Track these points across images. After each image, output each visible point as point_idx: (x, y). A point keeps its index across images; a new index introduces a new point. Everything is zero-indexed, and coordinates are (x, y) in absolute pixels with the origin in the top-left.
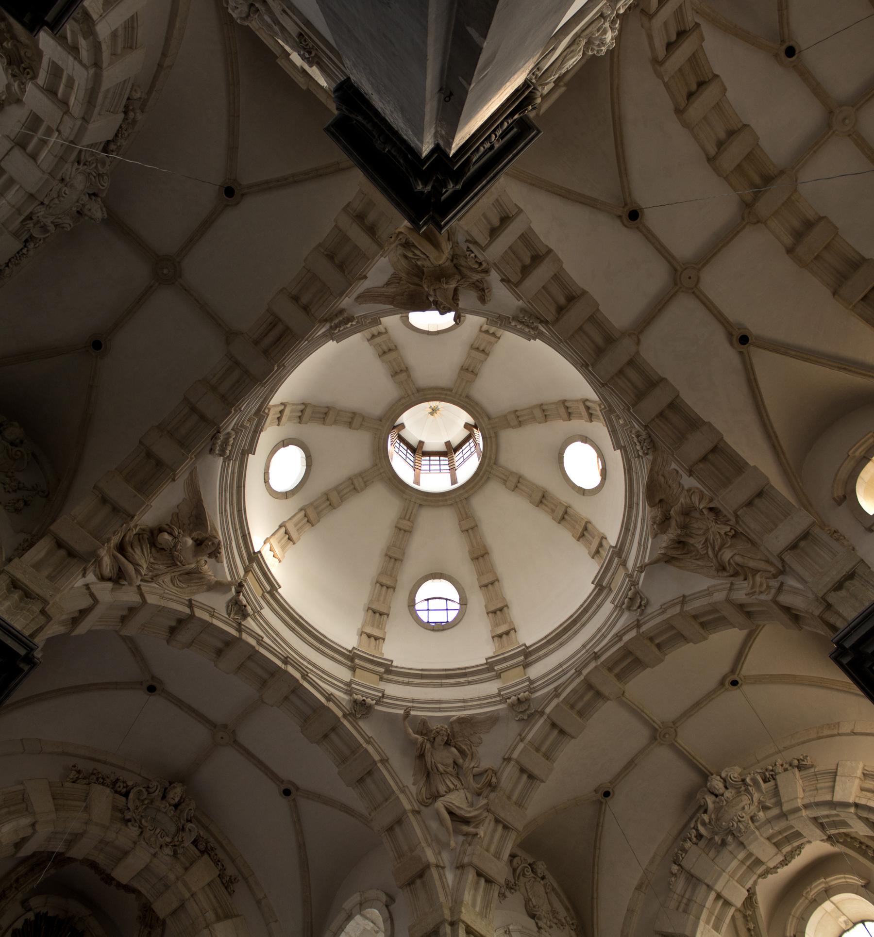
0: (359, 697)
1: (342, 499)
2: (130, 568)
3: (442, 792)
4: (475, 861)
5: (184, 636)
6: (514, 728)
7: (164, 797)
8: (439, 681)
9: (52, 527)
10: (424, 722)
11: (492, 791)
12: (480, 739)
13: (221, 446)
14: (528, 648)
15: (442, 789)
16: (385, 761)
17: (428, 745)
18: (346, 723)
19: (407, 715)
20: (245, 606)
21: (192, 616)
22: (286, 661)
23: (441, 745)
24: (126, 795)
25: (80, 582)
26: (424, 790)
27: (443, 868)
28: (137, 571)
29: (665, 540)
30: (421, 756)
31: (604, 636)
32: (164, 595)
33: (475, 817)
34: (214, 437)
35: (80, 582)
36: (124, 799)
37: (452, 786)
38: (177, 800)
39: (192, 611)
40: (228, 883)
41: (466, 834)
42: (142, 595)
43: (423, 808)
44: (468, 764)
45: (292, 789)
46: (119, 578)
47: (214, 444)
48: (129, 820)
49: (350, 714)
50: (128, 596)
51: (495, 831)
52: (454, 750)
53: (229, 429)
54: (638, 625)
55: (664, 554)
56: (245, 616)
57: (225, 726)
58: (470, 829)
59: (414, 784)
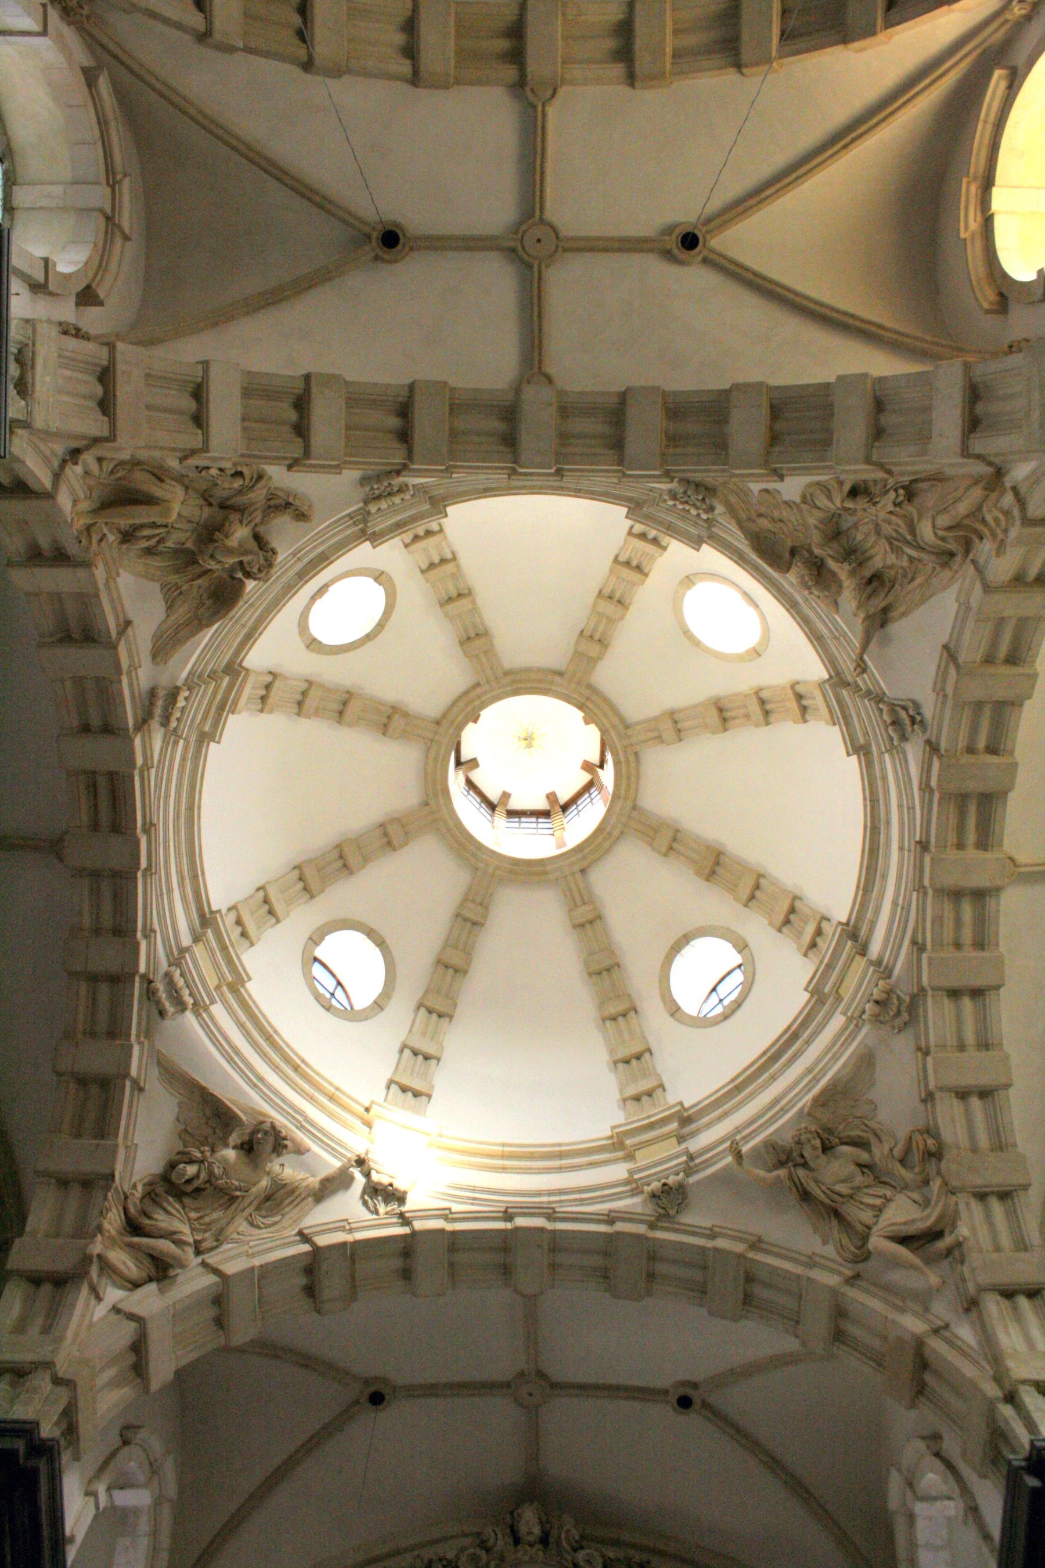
0: (656, 1185)
1: (468, 951)
2: (164, 1245)
4: (984, 1279)
5: (332, 1286)
6: (903, 1044)
7: (517, 1541)
8: (766, 1075)
9: (9, 1266)
10: (770, 1145)
11: (940, 1160)
12: (871, 1102)
13: (170, 996)
14: (847, 924)
15: (867, 1216)
16: (757, 1244)
17: (801, 1172)
18: (659, 1235)
19: (739, 1156)
20: (391, 1185)
21: (317, 1250)
22: (508, 1216)
23: (820, 1156)
25: (100, 1311)
26: (846, 1241)
27: (947, 1326)
28: (179, 1243)
29: (848, 598)
30: (805, 1196)
31: (911, 808)
32: (253, 1247)
33: (941, 1217)
34: (150, 993)
35: (100, 1311)
37: (878, 1202)
38: (537, 1531)
41: (949, 1252)
42: (216, 1271)
43: (861, 1266)
44: (879, 1152)
45: (690, 1392)
46: (161, 1270)
47: (158, 1002)
49: (659, 1217)
50: (192, 1282)
51: (988, 1216)
52: (846, 1149)
53: (164, 966)
54: (933, 747)
55: (868, 617)
56: (401, 1199)
57: (521, 1374)
58: (948, 1240)
59: (825, 1243)
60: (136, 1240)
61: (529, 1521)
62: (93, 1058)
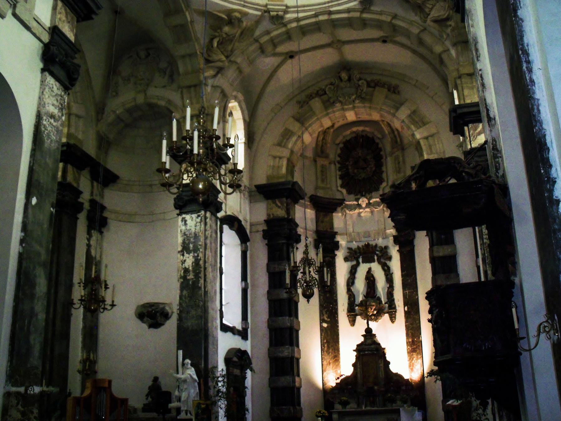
3: (428, 13)
16: (395, 17)
18: (365, 15)
20: (277, 15)
22: (316, 15)
24: (325, 93)
25: (209, 89)
26: (422, 16)
33: (448, 15)
35: (209, 89)
36: (326, 96)
38: (347, 78)
39: (260, 43)
40: (394, 90)
45: (385, 39)
48: (334, 102)
49: (364, 9)
56: (282, 18)
57: (333, 42)
60: (210, 65)
61: (344, 75)
62: (176, 20)
